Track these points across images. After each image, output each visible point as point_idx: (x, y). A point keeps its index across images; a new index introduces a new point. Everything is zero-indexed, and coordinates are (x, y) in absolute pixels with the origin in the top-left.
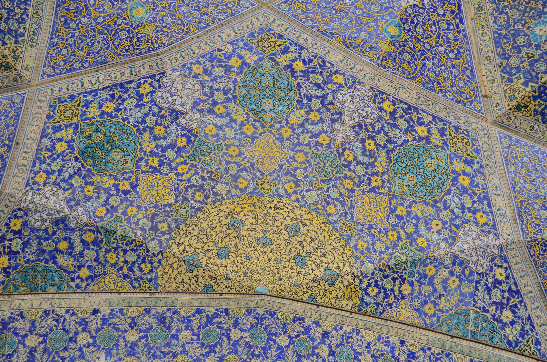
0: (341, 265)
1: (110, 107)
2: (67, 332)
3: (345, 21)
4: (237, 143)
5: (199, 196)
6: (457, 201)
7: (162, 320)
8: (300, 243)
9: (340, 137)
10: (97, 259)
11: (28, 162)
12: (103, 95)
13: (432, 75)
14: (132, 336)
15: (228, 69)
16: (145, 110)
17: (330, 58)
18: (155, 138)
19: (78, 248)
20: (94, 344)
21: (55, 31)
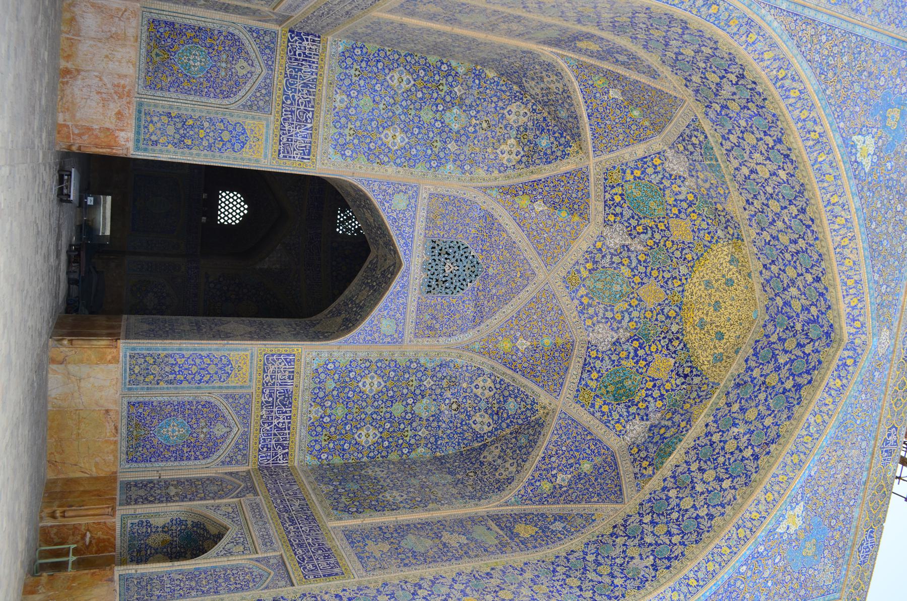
0: (725, 253)
1: (595, 375)
2: (706, 445)
3: (559, 238)
4: (643, 311)
5: (676, 343)
6: (653, 176)
7: (738, 385)
8: (717, 281)
9: (640, 248)
10: (682, 415)
11: (605, 429)
12: (585, 375)
13: (580, 194)
14: (735, 408)
15: (590, 305)
16: (606, 358)
17: (585, 248)
18: (627, 358)
19: (669, 423)
20: (723, 432)
21: (536, 383)
